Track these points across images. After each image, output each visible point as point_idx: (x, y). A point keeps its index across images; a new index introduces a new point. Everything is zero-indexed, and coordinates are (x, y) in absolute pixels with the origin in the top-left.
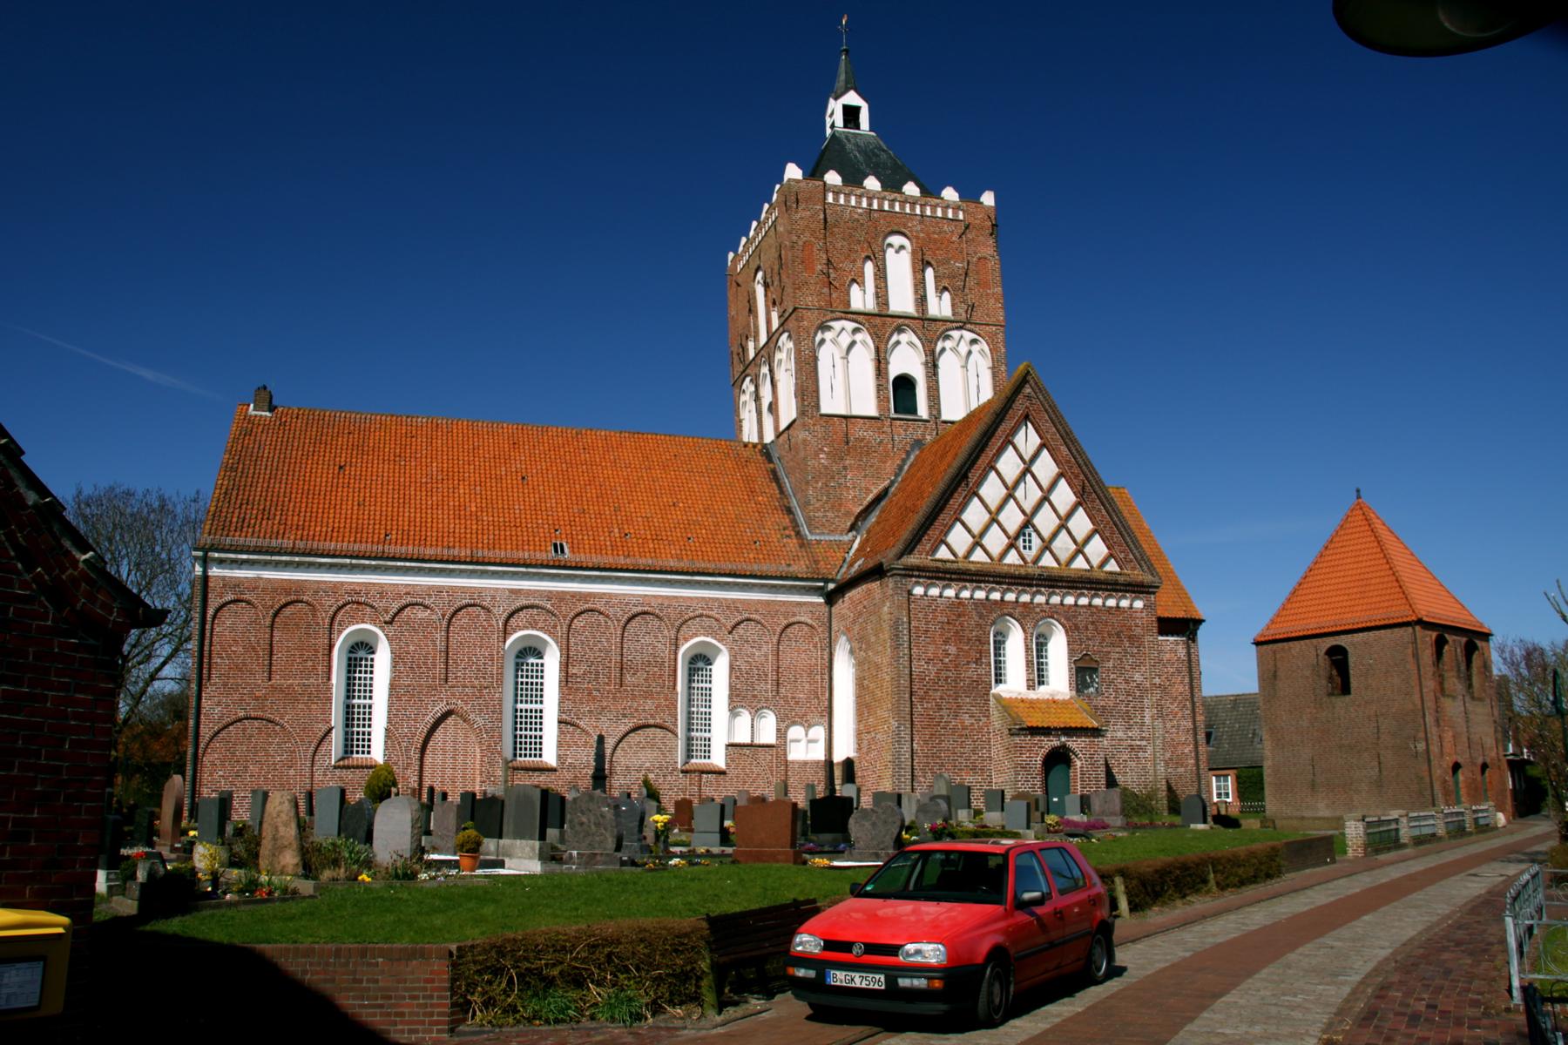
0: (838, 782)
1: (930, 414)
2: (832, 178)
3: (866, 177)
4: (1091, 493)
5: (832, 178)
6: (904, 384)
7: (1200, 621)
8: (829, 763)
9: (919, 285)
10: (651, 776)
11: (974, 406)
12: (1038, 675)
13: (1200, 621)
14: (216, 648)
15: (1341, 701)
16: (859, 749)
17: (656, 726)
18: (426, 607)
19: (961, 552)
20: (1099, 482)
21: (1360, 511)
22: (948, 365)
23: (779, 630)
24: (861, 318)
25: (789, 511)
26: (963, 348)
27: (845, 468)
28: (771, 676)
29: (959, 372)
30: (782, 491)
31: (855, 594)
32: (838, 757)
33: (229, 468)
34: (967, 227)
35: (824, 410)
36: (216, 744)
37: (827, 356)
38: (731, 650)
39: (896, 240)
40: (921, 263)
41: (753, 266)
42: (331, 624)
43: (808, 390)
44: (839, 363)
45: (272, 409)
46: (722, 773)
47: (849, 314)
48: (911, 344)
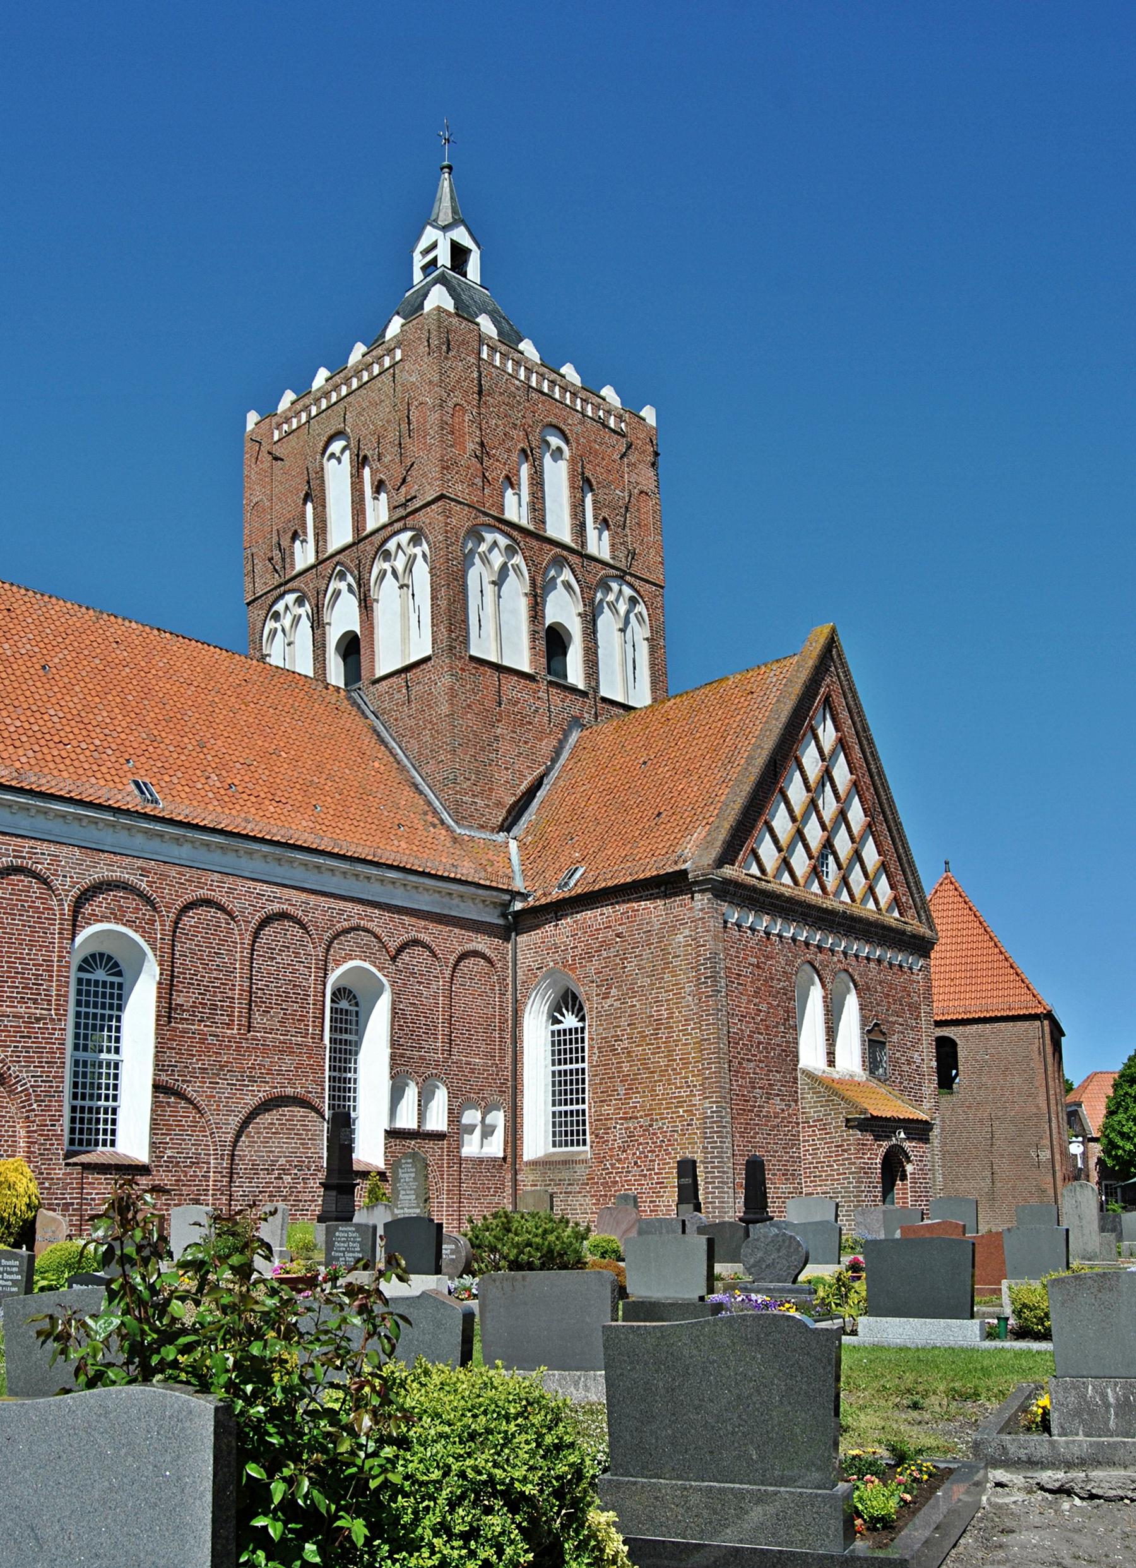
1: (588, 684)
4: (884, 820)
9: (577, 509)
22: (607, 623)
23: (452, 959)
37: (478, 576)
38: (393, 983)
41: (335, 425)
44: (489, 590)
48: (567, 586)
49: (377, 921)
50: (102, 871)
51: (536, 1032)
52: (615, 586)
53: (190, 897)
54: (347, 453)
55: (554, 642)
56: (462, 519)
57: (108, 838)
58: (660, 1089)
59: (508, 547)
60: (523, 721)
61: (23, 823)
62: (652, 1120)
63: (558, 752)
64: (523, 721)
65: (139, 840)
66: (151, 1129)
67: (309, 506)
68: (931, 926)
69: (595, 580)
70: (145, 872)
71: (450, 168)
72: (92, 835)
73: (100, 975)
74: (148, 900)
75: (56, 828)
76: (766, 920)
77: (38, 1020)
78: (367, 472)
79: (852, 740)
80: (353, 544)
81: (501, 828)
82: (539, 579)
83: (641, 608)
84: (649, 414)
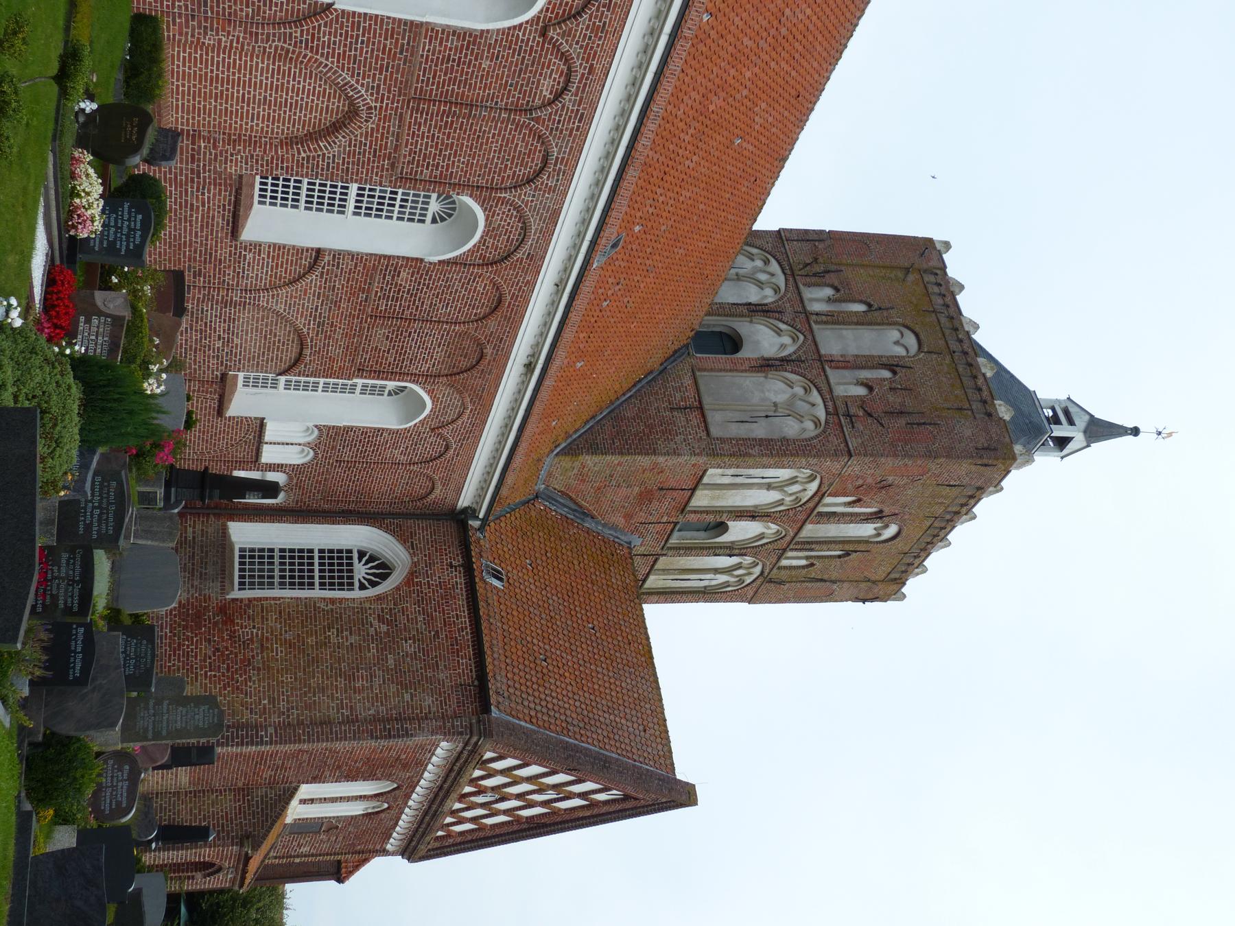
17: (301, 354)
18: (558, 95)
24: (811, 505)
54: (904, 353)
58: (288, 678)
62: (259, 669)
66: (275, 245)
67: (861, 308)
77: (393, 165)
78: (886, 374)
79: (596, 811)
80: (820, 356)
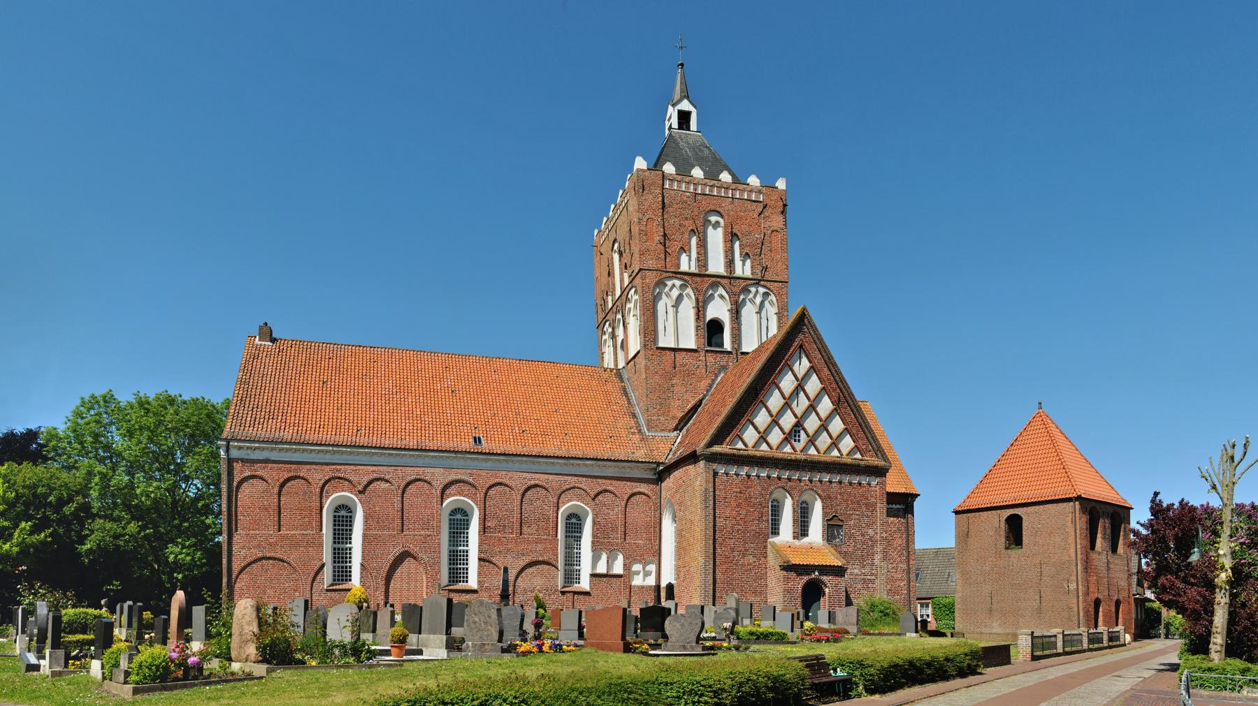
0: (663, 600)
2: (669, 168)
3: (693, 167)
5: (669, 168)
6: (715, 328)
7: (917, 495)
8: (658, 587)
9: (729, 253)
10: (541, 595)
11: (764, 339)
12: (802, 529)
13: (917, 495)
14: (240, 509)
15: (1015, 553)
16: (677, 578)
19: (751, 444)
20: (851, 395)
21: (1041, 417)
22: (748, 312)
23: (626, 497)
25: (634, 416)
26: (758, 300)
27: (673, 386)
28: (621, 529)
29: (755, 317)
30: (629, 403)
31: (677, 474)
32: (664, 584)
33: (242, 382)
34: (765, 207)
35: (661, 345)
36: (243, 576)
38: (593, 510)
39: (713, 219)
40: (731, 237)
42: (321, 492)
43: (649, 331)
44: (671, 310)
45: (274, 340)
46: (587, 594)
47: (678, 274)
48: (721, 297)
49: (584, 483)
50: (453, 477)
51: (668, 529)
52: (753, 289)
53: (492, 482)
55: (715, 328)
56: (652, 278)
57: (455, 463)
59: (681, 286)
60: (689, 374)
61: (420, 462)
63: (711, 386)
64: (689, 374)
65: (469, 462)
68: (885, 458)
69: (737, 289)
70: (471, 475)
71: (682, 65)
72: (448, 462)
73: (459, 516)
74: (474, 486)
75: (433, 462)
76: (746, 469)
81: (676, 429)
82: (701, 298)
83: (772, 297)
84: (781, 184)
